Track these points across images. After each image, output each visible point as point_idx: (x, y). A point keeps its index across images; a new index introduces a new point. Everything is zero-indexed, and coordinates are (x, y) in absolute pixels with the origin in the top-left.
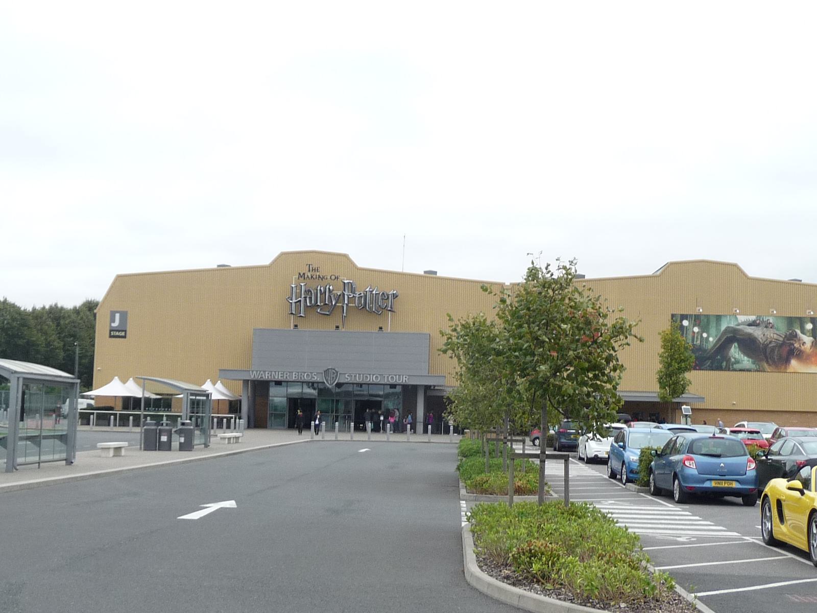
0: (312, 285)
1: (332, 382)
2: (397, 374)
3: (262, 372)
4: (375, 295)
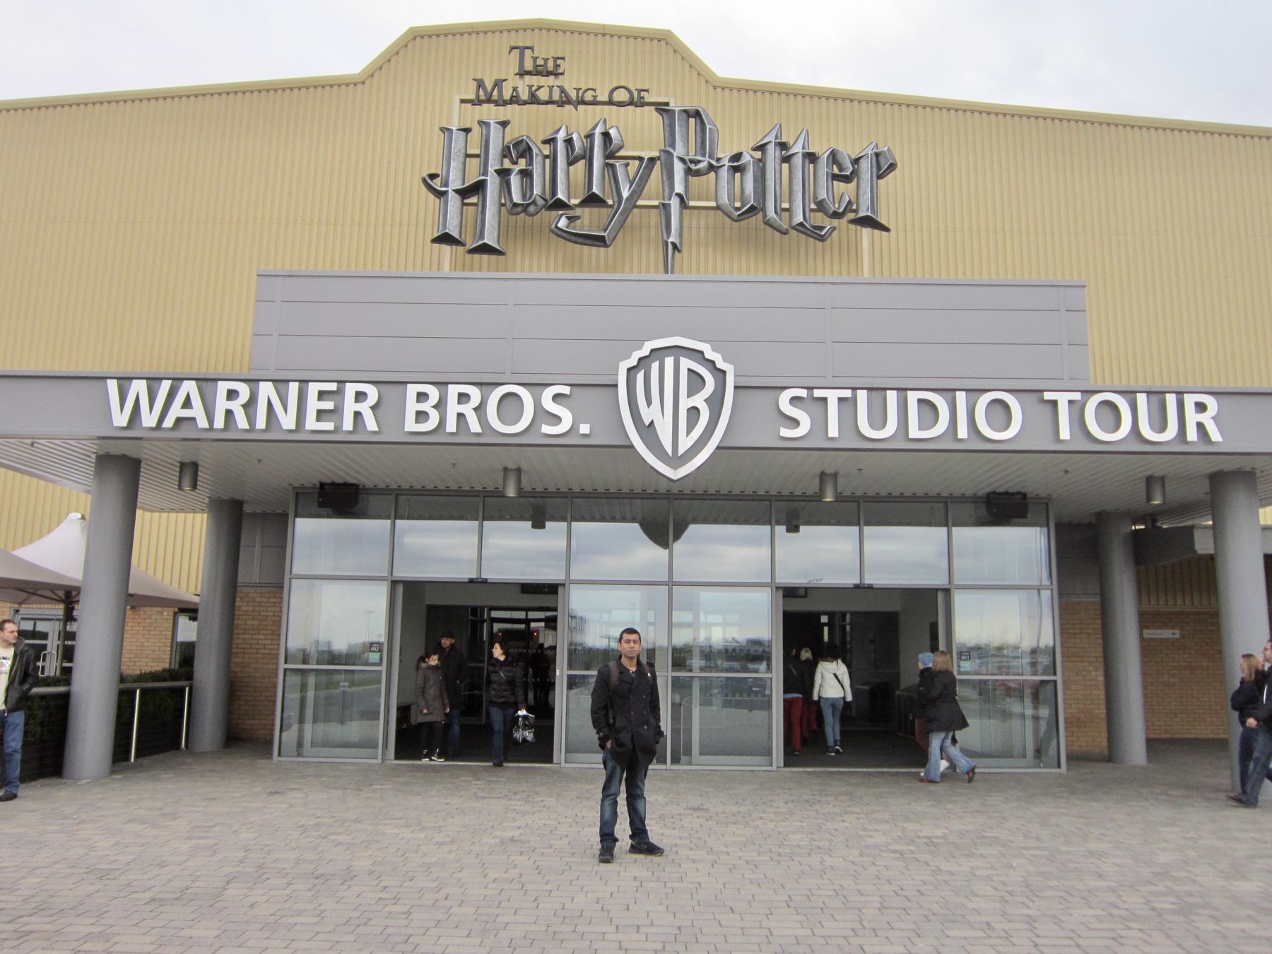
0: (528, 123)
1: (685, 443)
2: (1141, 384)
3: (189, 387)
4: (798, 161)
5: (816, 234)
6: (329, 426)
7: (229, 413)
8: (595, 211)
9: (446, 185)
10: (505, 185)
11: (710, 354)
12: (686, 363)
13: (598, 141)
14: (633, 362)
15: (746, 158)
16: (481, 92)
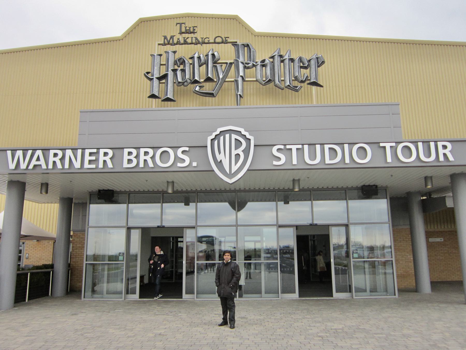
0: (184, 51)
1: (234, 168)
2: (420, 139)
3: (39, 153)
4: (287, 61)
5: (295, 89)
6: (93, 166)
7: (54, 162)
8: (211, 83)
9: (153, 76)
10: (175, 75)
11: (244, 132)
12: (234, 136)
13: (210, 57)
14: (213, 137)
15: (267, 61)
16: (166, 41)
